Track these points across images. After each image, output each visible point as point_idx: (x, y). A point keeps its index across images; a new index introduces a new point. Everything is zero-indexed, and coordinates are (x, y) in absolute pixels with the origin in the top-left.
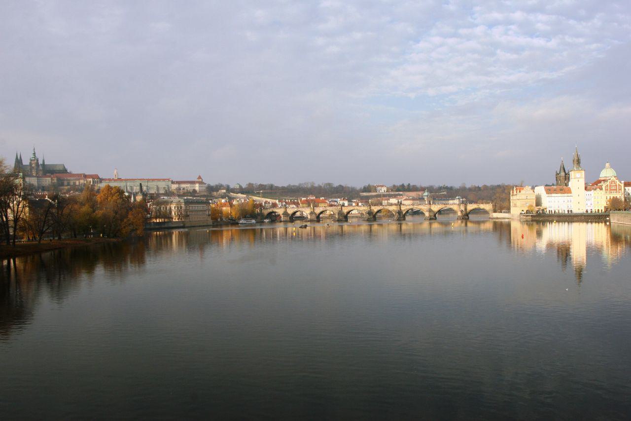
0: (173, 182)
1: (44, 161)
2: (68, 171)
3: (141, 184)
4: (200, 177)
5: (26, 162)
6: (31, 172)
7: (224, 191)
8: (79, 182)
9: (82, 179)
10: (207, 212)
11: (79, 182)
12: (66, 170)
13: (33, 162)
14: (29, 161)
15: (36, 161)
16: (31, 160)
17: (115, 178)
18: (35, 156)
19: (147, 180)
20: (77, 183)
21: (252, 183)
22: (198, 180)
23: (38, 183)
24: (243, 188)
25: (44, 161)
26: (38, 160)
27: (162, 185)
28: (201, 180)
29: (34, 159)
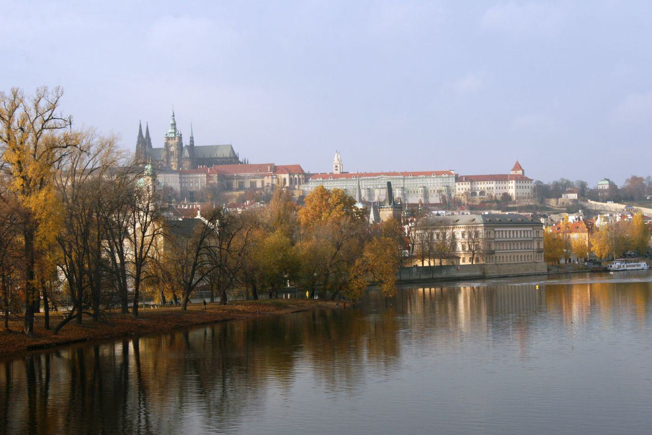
0: (458, 179)
1: (192, 138)
2: (241, 160)
3: (389, 184)
4: (518, 167)
5: (158, 142)
6: (168, 162)
7: (574, 196)
8: (263, 182)
9: (268, 176)
10: (536, 244)
11: (263, 182)
12: (236, 158)
13: (171, 142)
14: (164, 141)
15: (177, 141)
16: (168, 138)
17: (335, 172)
18: (175, 129)
19: (402, 174)
20: (259, 185)
21: (638, 176)
22: (513, 173)
23: (181, 187)
24: (619, 188)
25: (192, 141)
26: (180, 138)
27: (435, 184)
28: (520, 172)
29: (173, 135)
